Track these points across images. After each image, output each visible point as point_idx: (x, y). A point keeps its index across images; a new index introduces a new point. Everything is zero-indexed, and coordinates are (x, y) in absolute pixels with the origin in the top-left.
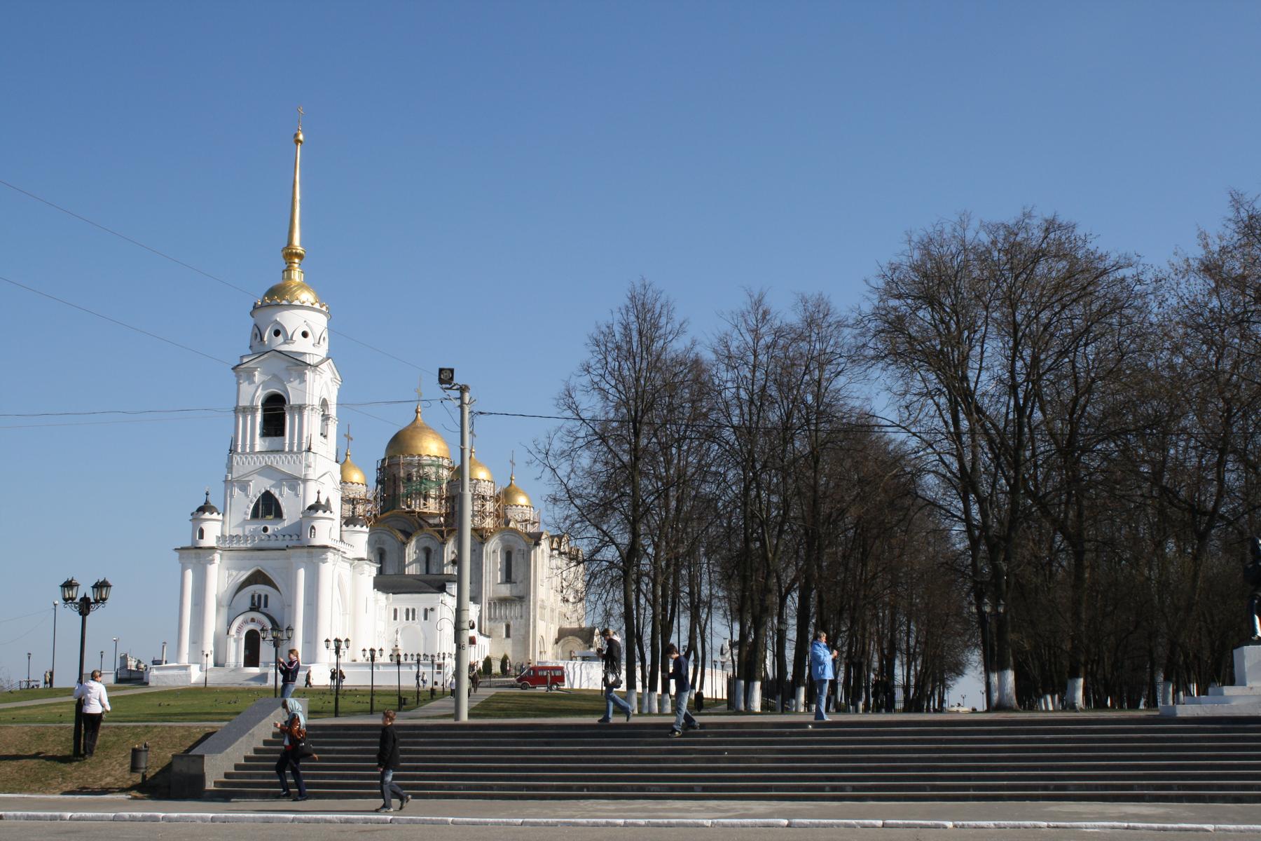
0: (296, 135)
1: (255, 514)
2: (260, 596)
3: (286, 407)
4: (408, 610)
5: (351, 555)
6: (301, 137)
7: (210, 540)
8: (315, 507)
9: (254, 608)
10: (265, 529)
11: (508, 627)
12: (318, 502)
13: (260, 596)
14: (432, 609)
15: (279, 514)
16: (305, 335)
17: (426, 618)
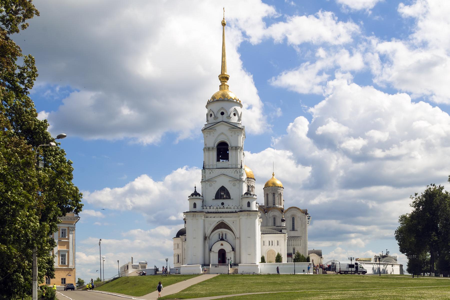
2: (222, 235)
3: (229, 148)
7: (199, 208)
9: (222, 239)
10: (223, 204)
13: (222, 235)
15: (228, 196)
16: (235, 115)
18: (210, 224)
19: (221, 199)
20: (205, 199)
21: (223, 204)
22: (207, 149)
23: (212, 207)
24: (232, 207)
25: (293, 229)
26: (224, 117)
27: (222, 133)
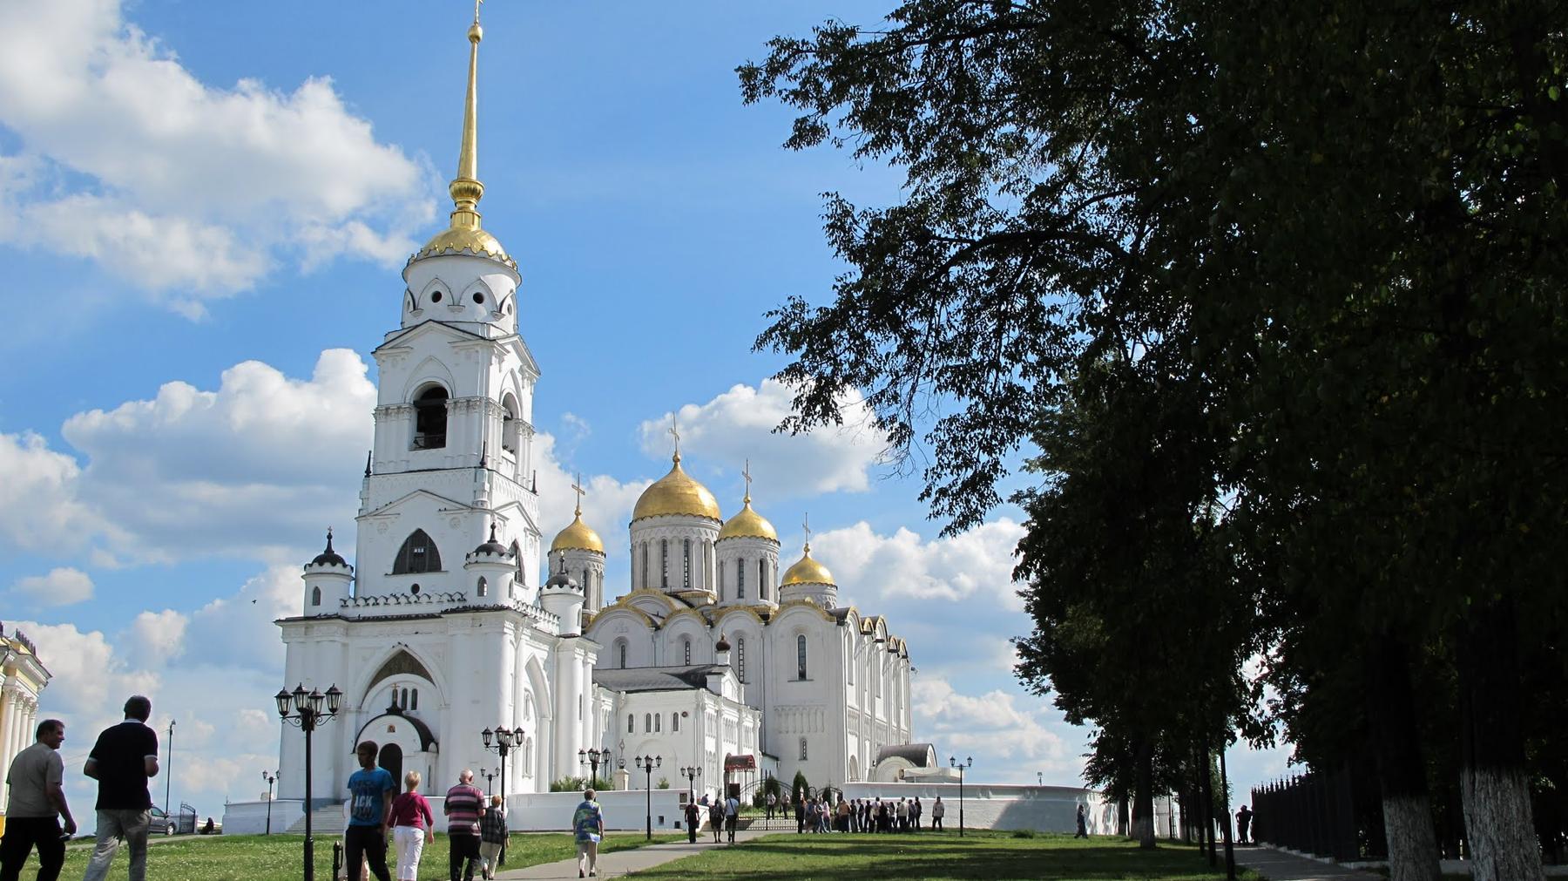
0: (474, 28)
1: (400, 568)
2: (405, 692)
3: (449, 404)
4: (648, 716)
5: (548, 626)
6: (480, 31)
8: (489, 548)
9: (394, 711)
10: (415, 589)
11: (804, 743)
12: (492, 539)
13: (405, 692)
14: (685, 714)
16: (478, 298)
17: (676, 728)
18: (365, 659)
19: (412, 570)
20: (361, 576)
21: (415, 589)
22: (383, 412)
23: (371, 601)
24: (435, 599)
25: (802, 676)
26: (440, 310)
27: (430, 359)
